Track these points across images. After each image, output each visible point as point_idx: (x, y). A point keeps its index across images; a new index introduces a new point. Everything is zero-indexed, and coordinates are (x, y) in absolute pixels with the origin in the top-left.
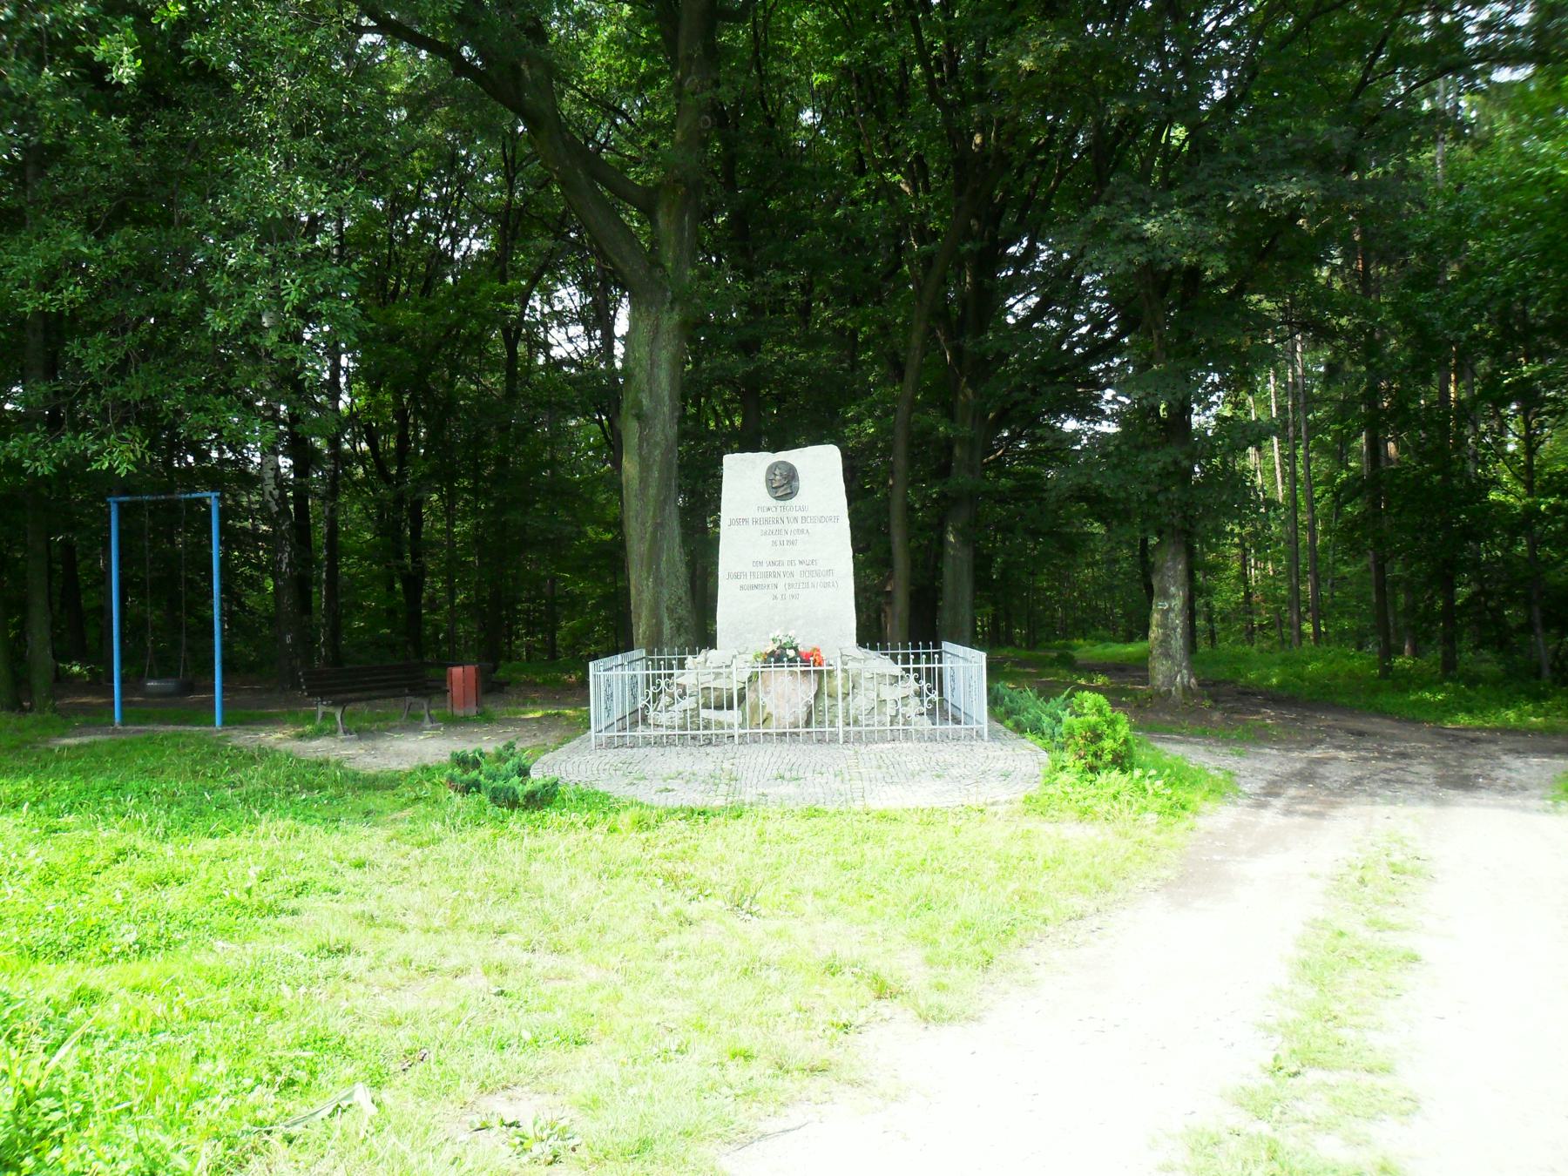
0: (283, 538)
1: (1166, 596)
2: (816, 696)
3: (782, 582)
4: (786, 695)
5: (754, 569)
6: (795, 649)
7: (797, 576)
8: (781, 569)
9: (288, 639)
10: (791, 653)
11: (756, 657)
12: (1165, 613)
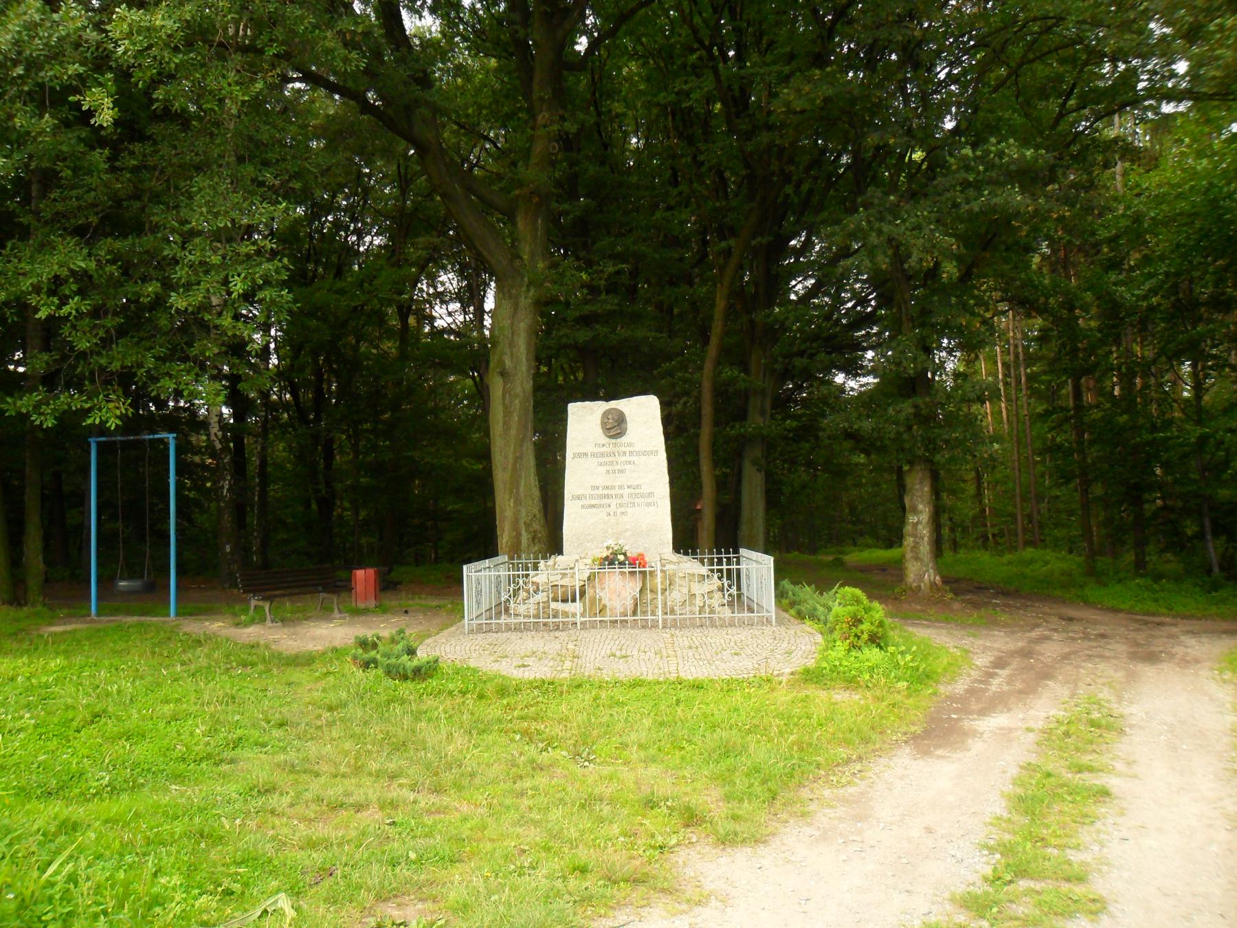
0: (225, 469)
1: (915, 511)
2: (641, 591)
3: (614, 502)
4: (618, 591)
6: (625, 554)
7: (626, 498)
8: (613, 492)
9: (228, 549)
10: (621, 558)
11: (594, 561)
12: (915, 525)
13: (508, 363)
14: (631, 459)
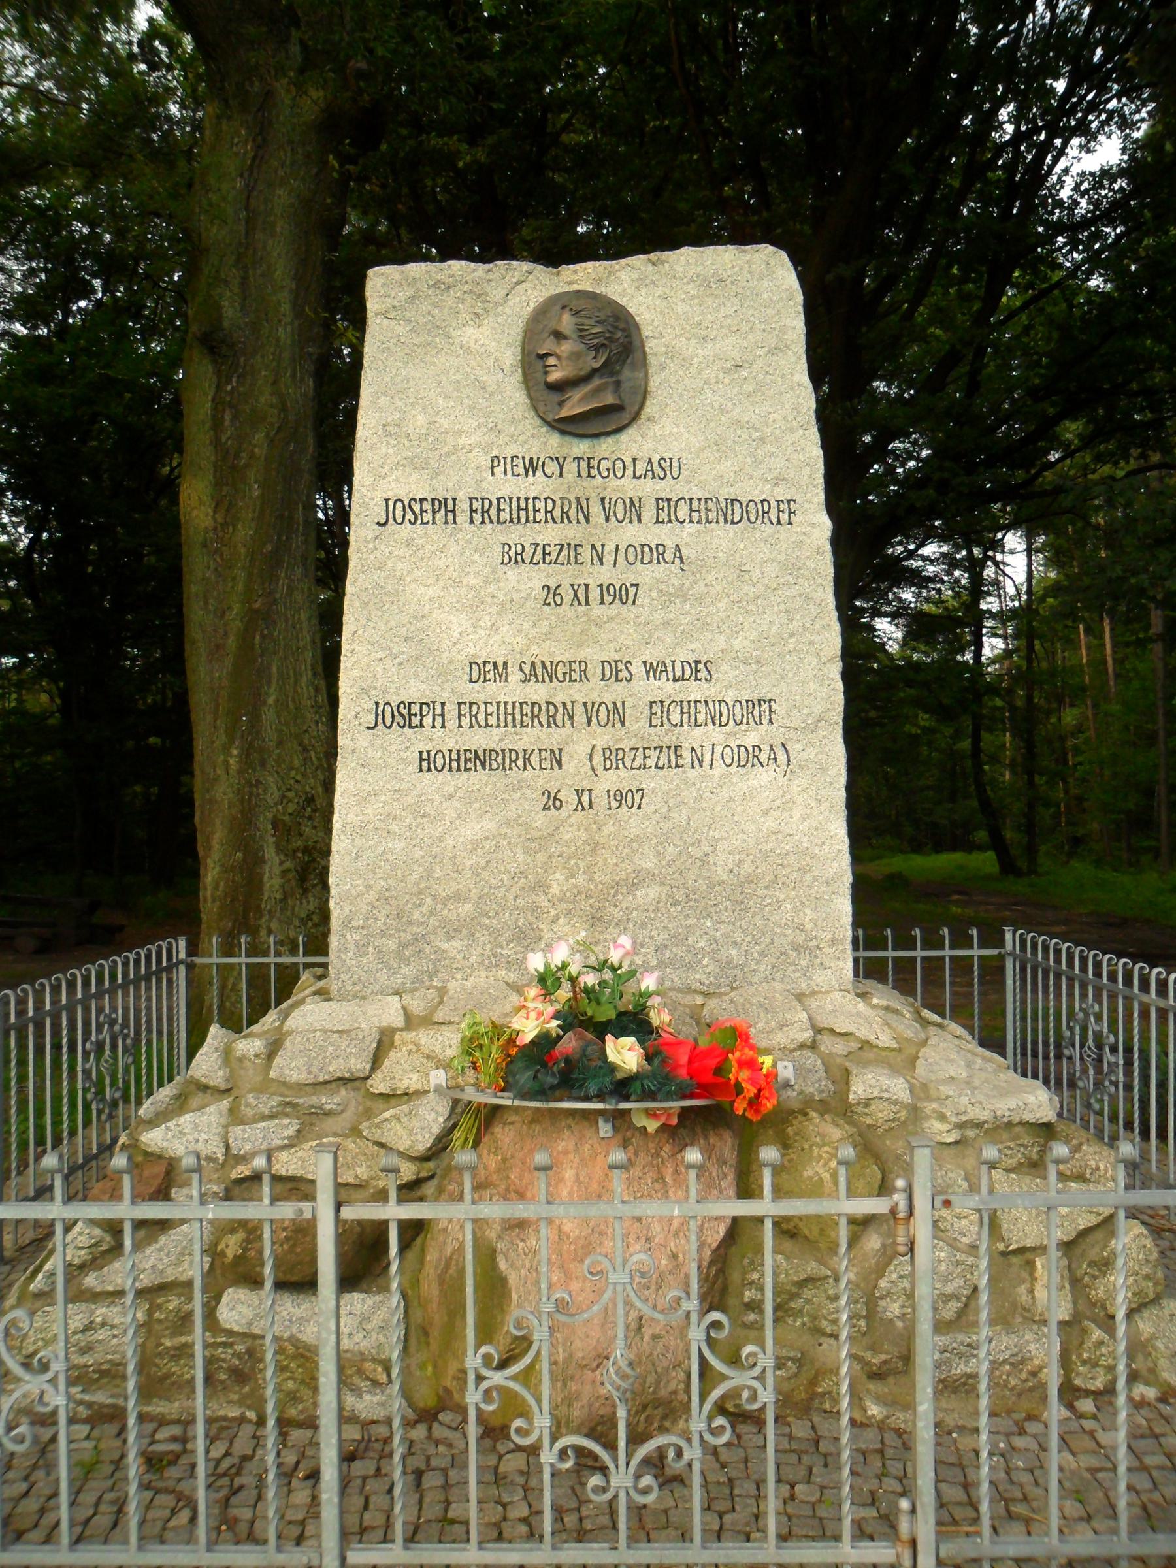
3: (580, 743)
4: (603, 1243)
5: (476, 692)
6: (633, 1021)
7: (637, 723)
8: (575, 693)
10: (625, 1053)
11: (472, 1045)
13: (230, 311)
14: (665, 535)
